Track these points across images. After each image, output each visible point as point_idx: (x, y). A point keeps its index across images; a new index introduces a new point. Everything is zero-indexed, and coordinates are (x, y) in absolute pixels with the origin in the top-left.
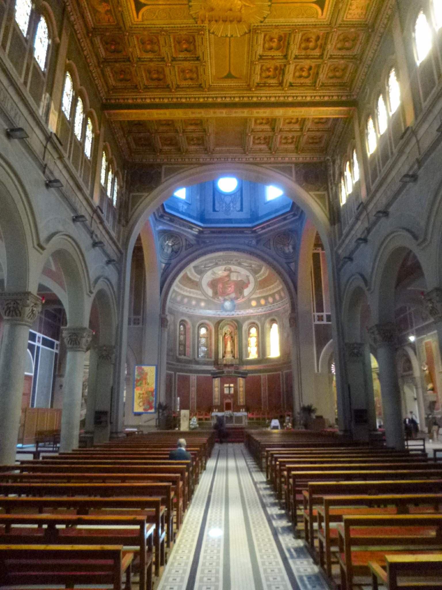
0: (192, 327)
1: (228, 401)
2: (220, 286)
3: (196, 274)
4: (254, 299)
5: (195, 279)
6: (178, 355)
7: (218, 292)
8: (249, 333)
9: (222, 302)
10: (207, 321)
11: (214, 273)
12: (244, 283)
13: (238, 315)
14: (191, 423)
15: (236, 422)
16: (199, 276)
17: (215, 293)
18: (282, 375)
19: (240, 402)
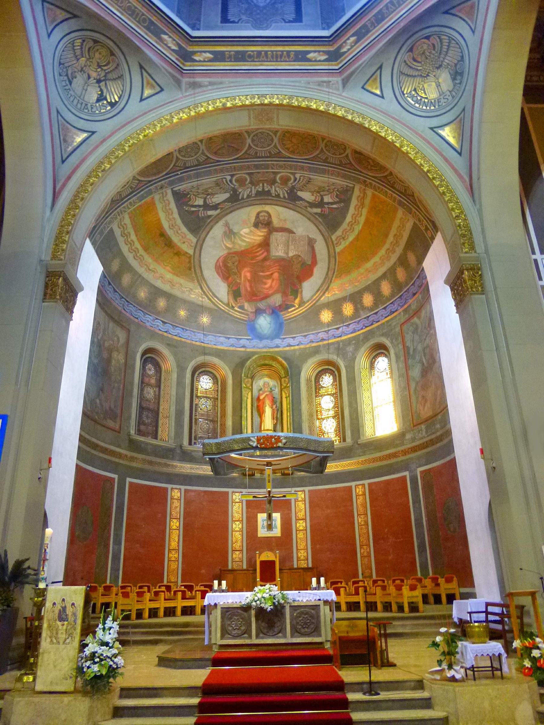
0: (175, 369)
1: (267, 556)
2: (246, 273)
3: (184, 229)
4: (327, 305)
5: (184, 247)
6: (132, 432)
7: (243, 292)
8: (318, 387)
9: (252, 316)
10: (215, 360)
11: (230, 233)
12: (303, 264)
13: (290, 346)
14: (92, 647)
15: (295, 631)
16: (194, 240)
17: (236, 294)
18: (414, 480)
19: (298, 559)
